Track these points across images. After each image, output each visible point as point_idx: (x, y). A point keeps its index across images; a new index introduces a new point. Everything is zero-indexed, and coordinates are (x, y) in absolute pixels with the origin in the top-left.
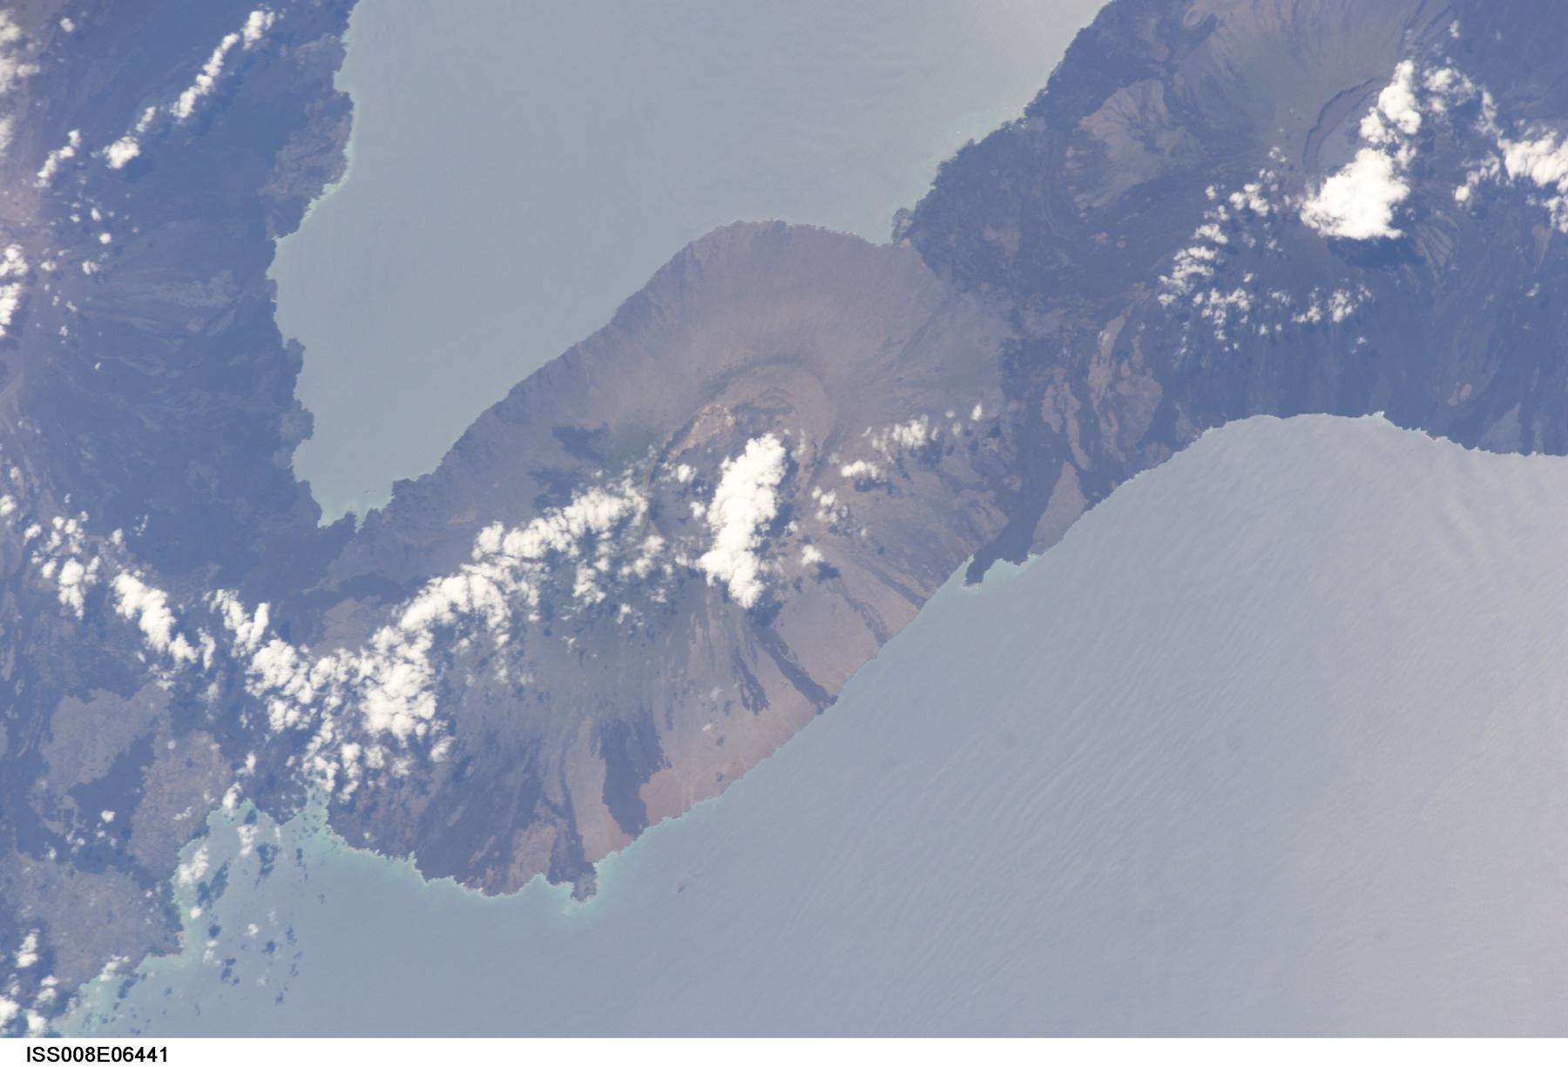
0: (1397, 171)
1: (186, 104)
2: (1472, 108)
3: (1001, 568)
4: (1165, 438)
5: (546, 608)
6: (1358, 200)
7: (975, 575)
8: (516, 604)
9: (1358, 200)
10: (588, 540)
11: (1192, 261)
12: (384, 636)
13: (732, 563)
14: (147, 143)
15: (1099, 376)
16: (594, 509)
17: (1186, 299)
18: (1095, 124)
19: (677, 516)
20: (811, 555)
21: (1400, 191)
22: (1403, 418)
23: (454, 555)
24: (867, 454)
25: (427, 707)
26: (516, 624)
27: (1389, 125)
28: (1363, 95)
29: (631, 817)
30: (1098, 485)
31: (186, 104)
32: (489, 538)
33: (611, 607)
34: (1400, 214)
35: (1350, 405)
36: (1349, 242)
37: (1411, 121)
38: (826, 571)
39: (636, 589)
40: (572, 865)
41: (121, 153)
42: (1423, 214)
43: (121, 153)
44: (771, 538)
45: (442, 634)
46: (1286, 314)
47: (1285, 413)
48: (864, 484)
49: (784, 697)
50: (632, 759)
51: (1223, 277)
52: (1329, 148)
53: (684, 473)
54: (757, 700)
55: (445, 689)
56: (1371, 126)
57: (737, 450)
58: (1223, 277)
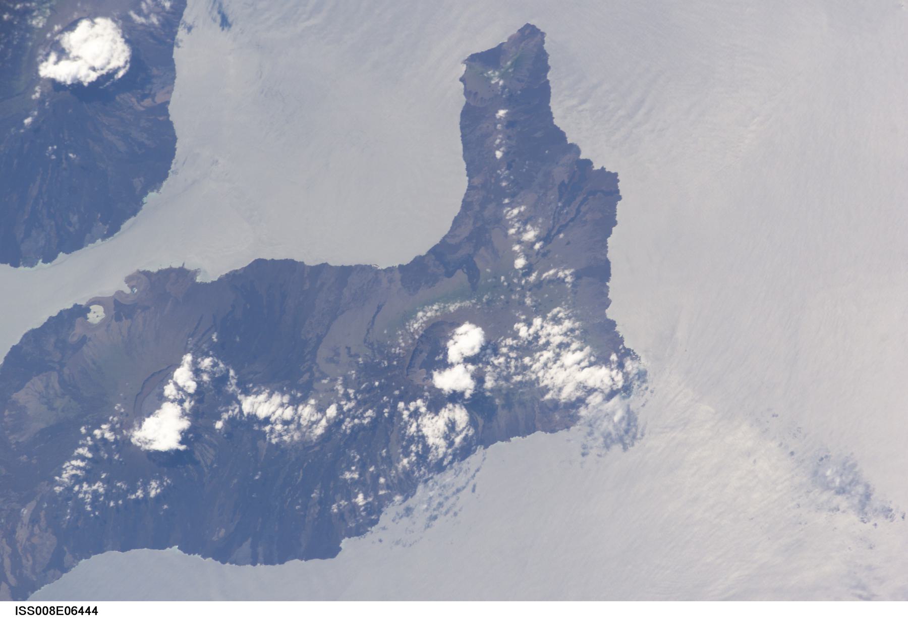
0: (184, 414)
2: (224, 378)
9: (163, 430)
11: (72, 468)
17: (69, 489)
21: (185, 424)
22: (188, 549)
27: (179, 389)
28: (166, 375)
34: (185, 437)
35: (159, 543)
36: (158, 453)
37: (192, 386)
42: (198, 437)
46: (123, 494)
47: (124, 549)
51: (90, 476)
52: (147, 402)
56: (170, 390)
58: (90, 476)
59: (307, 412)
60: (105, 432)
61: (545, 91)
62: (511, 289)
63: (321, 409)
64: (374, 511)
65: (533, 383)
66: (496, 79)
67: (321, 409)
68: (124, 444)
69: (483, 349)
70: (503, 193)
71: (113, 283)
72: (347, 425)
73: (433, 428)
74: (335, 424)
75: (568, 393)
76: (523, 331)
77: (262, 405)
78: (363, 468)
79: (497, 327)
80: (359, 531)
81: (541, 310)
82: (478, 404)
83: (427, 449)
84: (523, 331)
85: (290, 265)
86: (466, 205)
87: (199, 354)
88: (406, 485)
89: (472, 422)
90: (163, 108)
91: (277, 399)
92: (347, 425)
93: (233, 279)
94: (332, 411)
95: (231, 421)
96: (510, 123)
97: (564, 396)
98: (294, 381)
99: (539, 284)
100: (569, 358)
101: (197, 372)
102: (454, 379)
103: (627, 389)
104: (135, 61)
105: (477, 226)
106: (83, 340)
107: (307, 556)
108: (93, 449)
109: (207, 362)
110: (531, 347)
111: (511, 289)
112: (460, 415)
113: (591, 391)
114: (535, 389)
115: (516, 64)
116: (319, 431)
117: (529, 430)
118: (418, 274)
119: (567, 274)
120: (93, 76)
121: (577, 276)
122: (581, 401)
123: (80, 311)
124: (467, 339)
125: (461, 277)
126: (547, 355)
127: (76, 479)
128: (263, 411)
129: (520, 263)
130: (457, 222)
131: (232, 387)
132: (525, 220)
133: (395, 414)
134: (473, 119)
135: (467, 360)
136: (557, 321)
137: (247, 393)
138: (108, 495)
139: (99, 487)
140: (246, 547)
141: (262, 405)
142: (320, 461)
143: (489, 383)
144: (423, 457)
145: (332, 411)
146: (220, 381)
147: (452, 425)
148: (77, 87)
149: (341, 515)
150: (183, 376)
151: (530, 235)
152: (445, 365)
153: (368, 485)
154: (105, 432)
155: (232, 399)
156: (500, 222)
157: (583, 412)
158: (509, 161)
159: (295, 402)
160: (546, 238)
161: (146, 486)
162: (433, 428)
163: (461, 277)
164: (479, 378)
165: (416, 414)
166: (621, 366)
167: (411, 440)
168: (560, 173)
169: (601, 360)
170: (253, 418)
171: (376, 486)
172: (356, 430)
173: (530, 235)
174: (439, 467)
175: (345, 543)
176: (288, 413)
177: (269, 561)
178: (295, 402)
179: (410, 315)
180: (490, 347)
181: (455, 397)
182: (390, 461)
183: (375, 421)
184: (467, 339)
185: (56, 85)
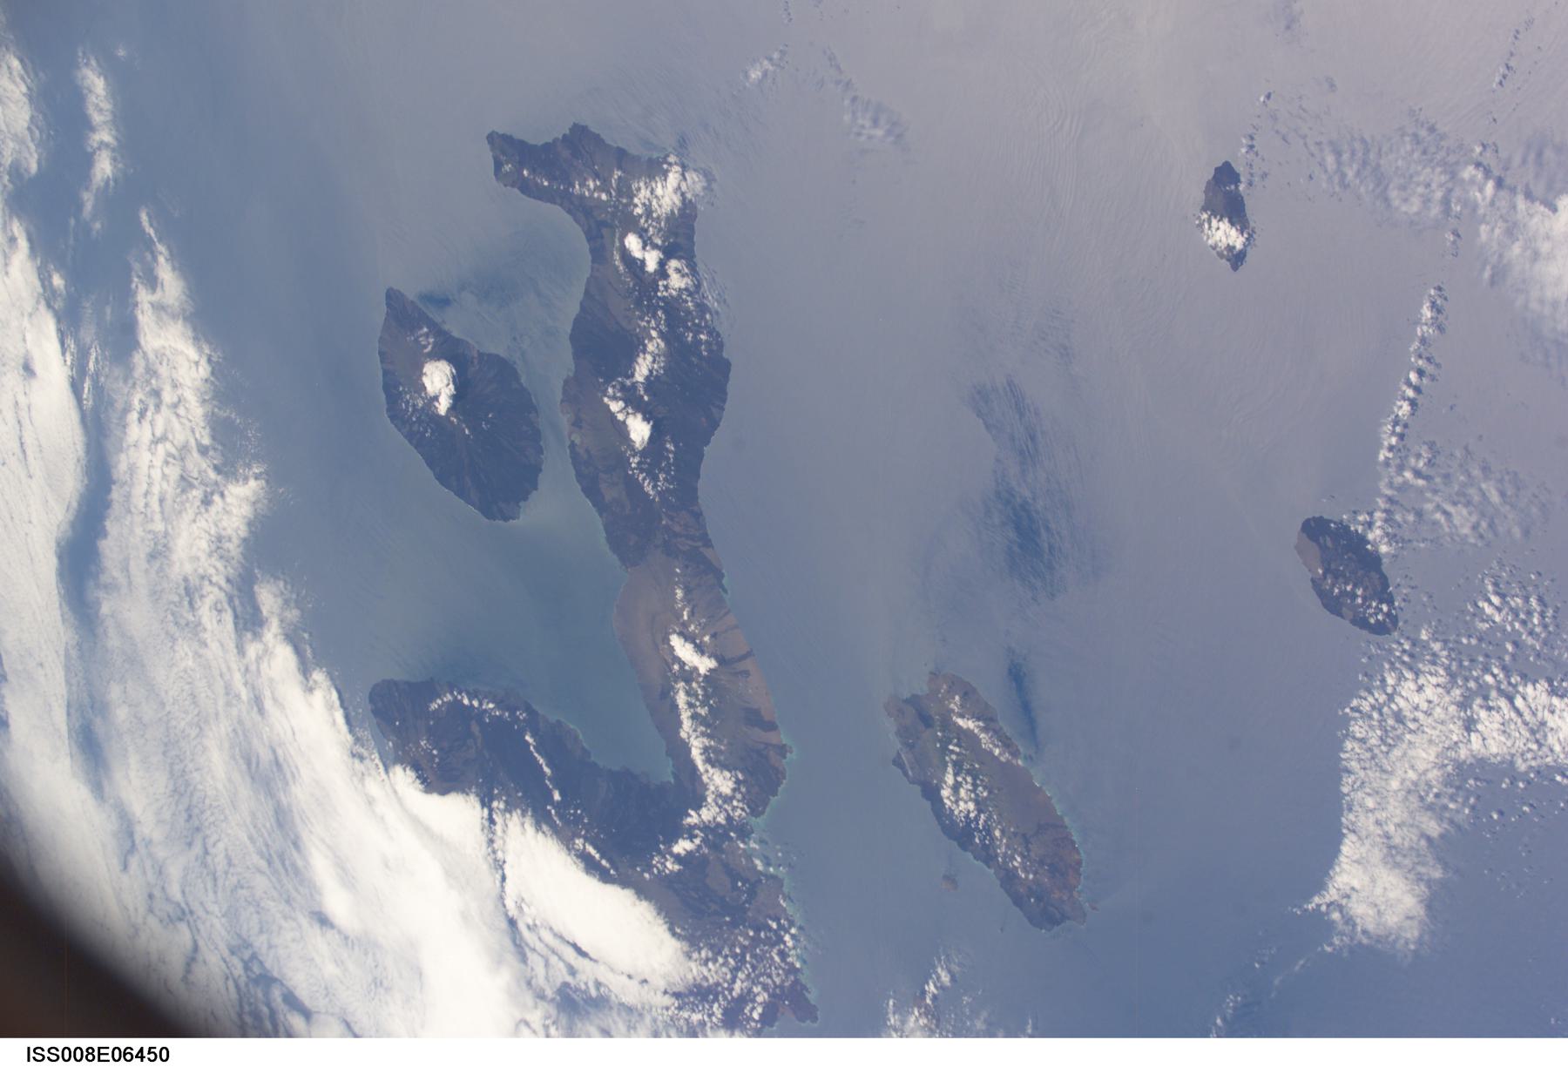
1: (547, 770)
3: (725, 581)
4: (698, 515)
5: (708, 726)
6: (639, 430)
7: (725, 591)
8: (703, 734)
10: (690, 705)
11: (648, 487)
12: (705, 778)
13: (704, 664)
14: (556, 786)
15: (677, 529)
16: (681, 699)
17: (659, 493)
18: (608, 498)
19: (689, 675)
20: (707, 639)
21: (639, 416)
23: (686, 748)
24: (683, 609)
25: (728, 774)
26: (709, 736)
28: (612, 416)
29: (771, 727)
30: (708, 543)
31: (547, 770)
32: (683, 735)
33: (710, 707)
35: (701, 456)
36: (651, 438)
37: (621, 404)
38: (714, 636)
39: (706, 696)
40: (782, 750)
41: (557, 796)
43: (557, 796)
44: (700, 649)
45: (708, 761)
46: (669, 465)
47: (698, 476)
48: (692, 614)
49: (747, 665)
50: (754, 718)
51: (655, 479)
52: (622, 430)
53: (676, 667)
54: (746, 673)
55: (724, 766)
56: (620, 417)
57: (672, 649)
58: (655, 479)
59: (651, 347)
60: (634, 461)
61: (522, 143)
62: (616, 207)
63: (651, 339)
64: (712, 332)
65: (668, 219)
66: (508, 167)
67: (651, 339)
68: (644, 453)
69: (641, 237)
70: (566, 190)
71: (564, 420)
72: (663, 327)
73: (677, 282)
74: (662, 335)
75: (677, 200)
76: (639, 211)
77: (642, 369)
78: (688, 329)
79: (631, 224)
80: (721, 345)
81: (631, 196)
82: (669, 252)
83: (686, 289)
84: (639, 211)
85: (577, 321)
86: (569, 212)
87: (605, 393)
88: (702, 308)
89: (679, 258)
90: (481, 355)
91: (640, 360)
92: (663, 327)
93: (577, 355)
94: (654, 334)
95: (646, 391)
96: (533, 171)
97: (678, 203)
98: (634, 347)
99: (620, 193)
100: (659, 191)
101: (614, 398)
102: (652, 260)
103: (684, 167)
104: (451, 360)
105: (582, 210)
106: (587, 451)
107: (727, 378)
108: (642, 471)
109: (610, 390)
110: (649, 211)
111: (616, 207)
112: (674, 264)
113: (679, 187)
114: (670, 218)
115: (504, 153)
116: (662, 345)
117: (692, 228)
118: (599, 254)
119: (617, 174)
120: (452, 386)
121: (620, 168)
122: (683, 194)
123: (573, 445)
124: (633, 243)
125: (605, 231)
126: (654, 203)
127: (655, 487)
128: (646, 372)
129: (604, 197)
130: (577, 221)
131: (628, 383)
132: (583, 185)
133: (663, 299)
134: (526, 188)
135: (644, 248)
136: (639, 189)
137: (633, 375)
138: (668, 473)
139: (662, 476)
140: (714, 410)
141: (642, 369)
142: (678, 351)
143: (659, 242)
144: (690, 294)
145: (654, 334)
146: (623, 388)
147: (678, 271)
148: (456, 399)
149: (710, 351)
150: (615, 407)
151: (591, 184)
152: (643, 262)
153: (697, 330)
154: (634, 461)
155: (634, 385)
156: (582, 197)
157: (689, 196)
158: (551, 179)
159: (644, 351)
160: (597, 176)
161: (668, 451)
162: (677, 282)
163: (605, 231)
164: (655, 247)
165: (666, 287)
166: (670, 164)
167: (680, 296)
168: (566, 154)
169: (665, 174)
170: (647, 378)
171: (699, 325)
172: (668, 324)
173: (591, 184)
174: (698, 286)
175: (725, 355)
176: (649, 358)
177: (724, 401)
178: (644, 351)
179: (616, 268)
180: (642, 233)
181: (662, 264)
182: (688, 312)
183: (665, 312)
184: (633, 243)
185: (452, 409)
